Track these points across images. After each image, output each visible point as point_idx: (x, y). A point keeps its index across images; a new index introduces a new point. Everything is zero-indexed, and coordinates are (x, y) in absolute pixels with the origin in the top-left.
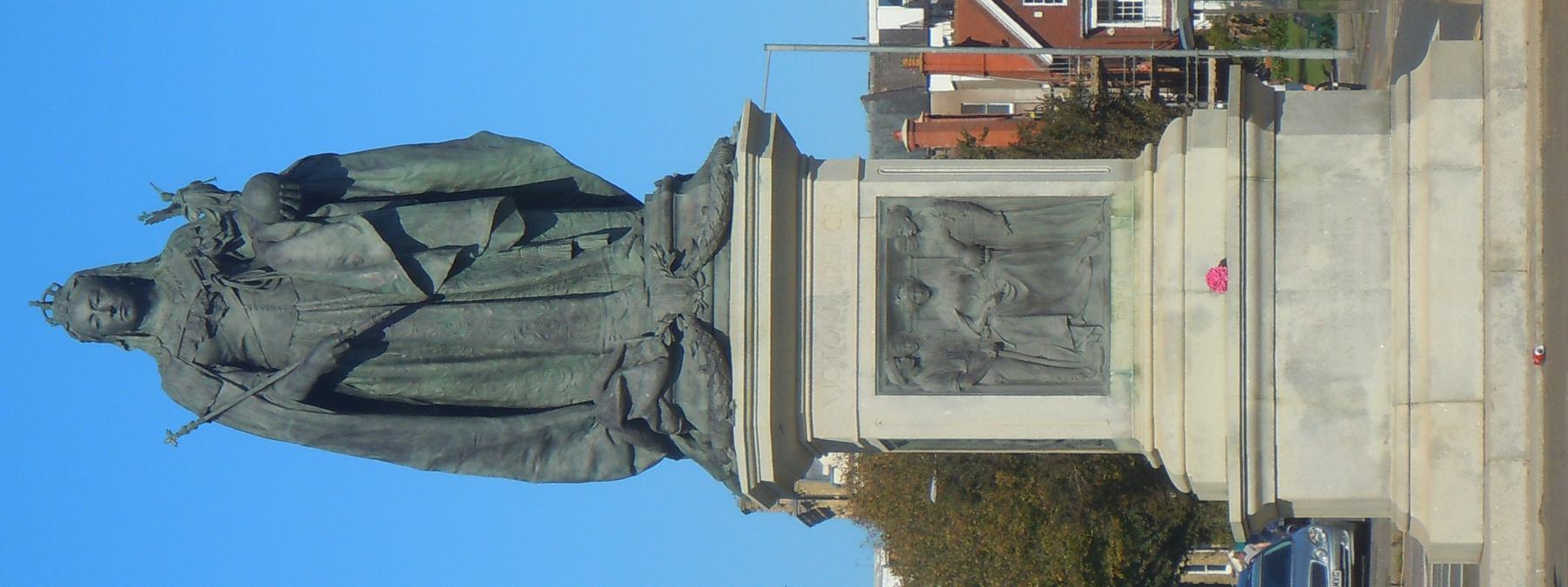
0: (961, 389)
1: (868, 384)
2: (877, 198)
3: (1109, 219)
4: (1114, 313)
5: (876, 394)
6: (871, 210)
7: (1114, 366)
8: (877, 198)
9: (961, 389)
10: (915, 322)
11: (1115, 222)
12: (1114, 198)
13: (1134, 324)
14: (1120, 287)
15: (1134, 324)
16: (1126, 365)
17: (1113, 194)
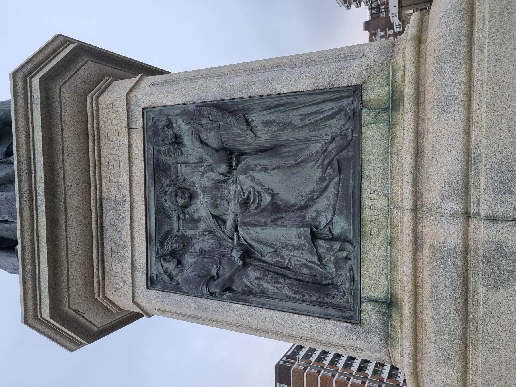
0: (211, 294)
1: (141, 279)
2: (143, 109)
3: (360, 113)
4: (366, 229)
5: (148, 288)
6: (138, 122)
7: (366, 292)
8: (143, 109)
9: (211, 294)
10: (181, 224)
11: (367, 117)
12: (367, 86)
13: (390, 242)
14: (373, 196)
15: (390, 242)
16: (381, 293)
17: (364, 83)
